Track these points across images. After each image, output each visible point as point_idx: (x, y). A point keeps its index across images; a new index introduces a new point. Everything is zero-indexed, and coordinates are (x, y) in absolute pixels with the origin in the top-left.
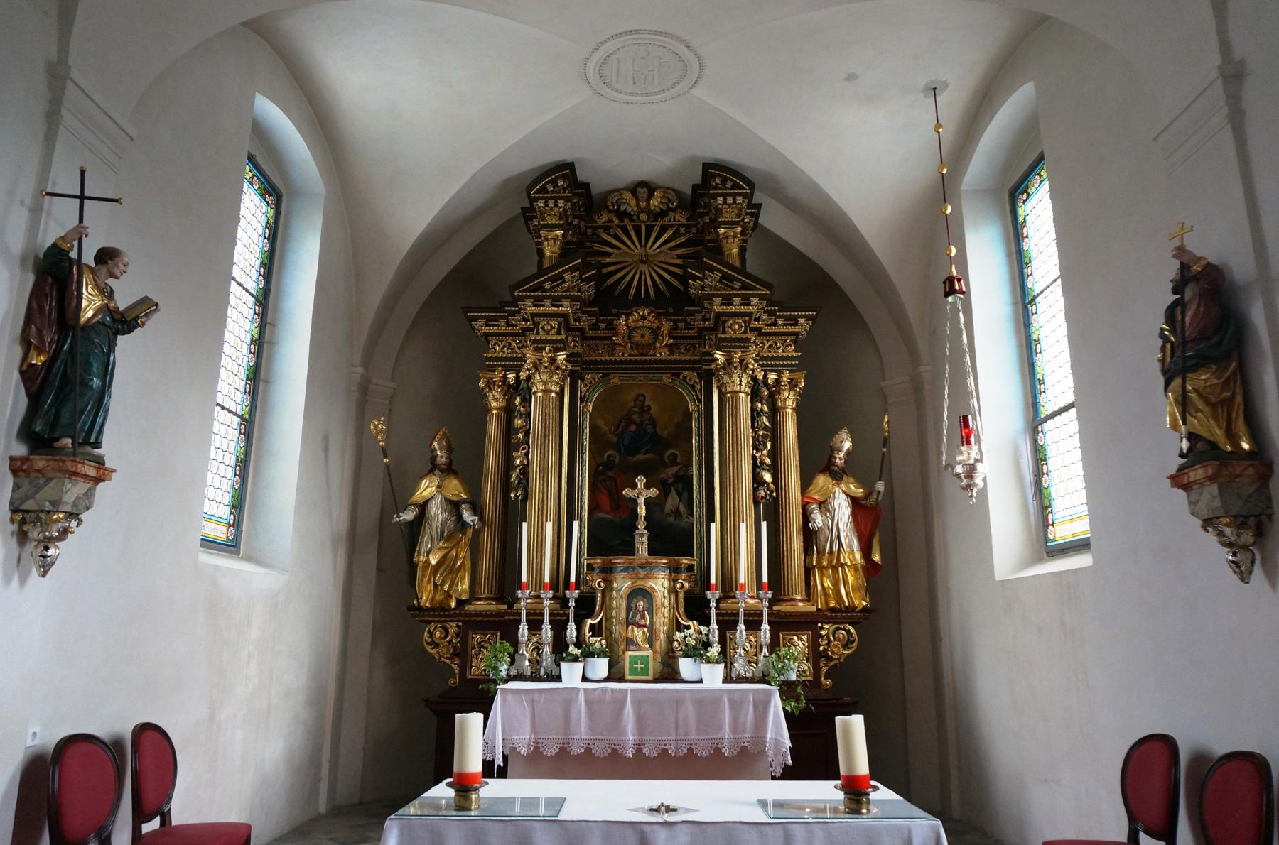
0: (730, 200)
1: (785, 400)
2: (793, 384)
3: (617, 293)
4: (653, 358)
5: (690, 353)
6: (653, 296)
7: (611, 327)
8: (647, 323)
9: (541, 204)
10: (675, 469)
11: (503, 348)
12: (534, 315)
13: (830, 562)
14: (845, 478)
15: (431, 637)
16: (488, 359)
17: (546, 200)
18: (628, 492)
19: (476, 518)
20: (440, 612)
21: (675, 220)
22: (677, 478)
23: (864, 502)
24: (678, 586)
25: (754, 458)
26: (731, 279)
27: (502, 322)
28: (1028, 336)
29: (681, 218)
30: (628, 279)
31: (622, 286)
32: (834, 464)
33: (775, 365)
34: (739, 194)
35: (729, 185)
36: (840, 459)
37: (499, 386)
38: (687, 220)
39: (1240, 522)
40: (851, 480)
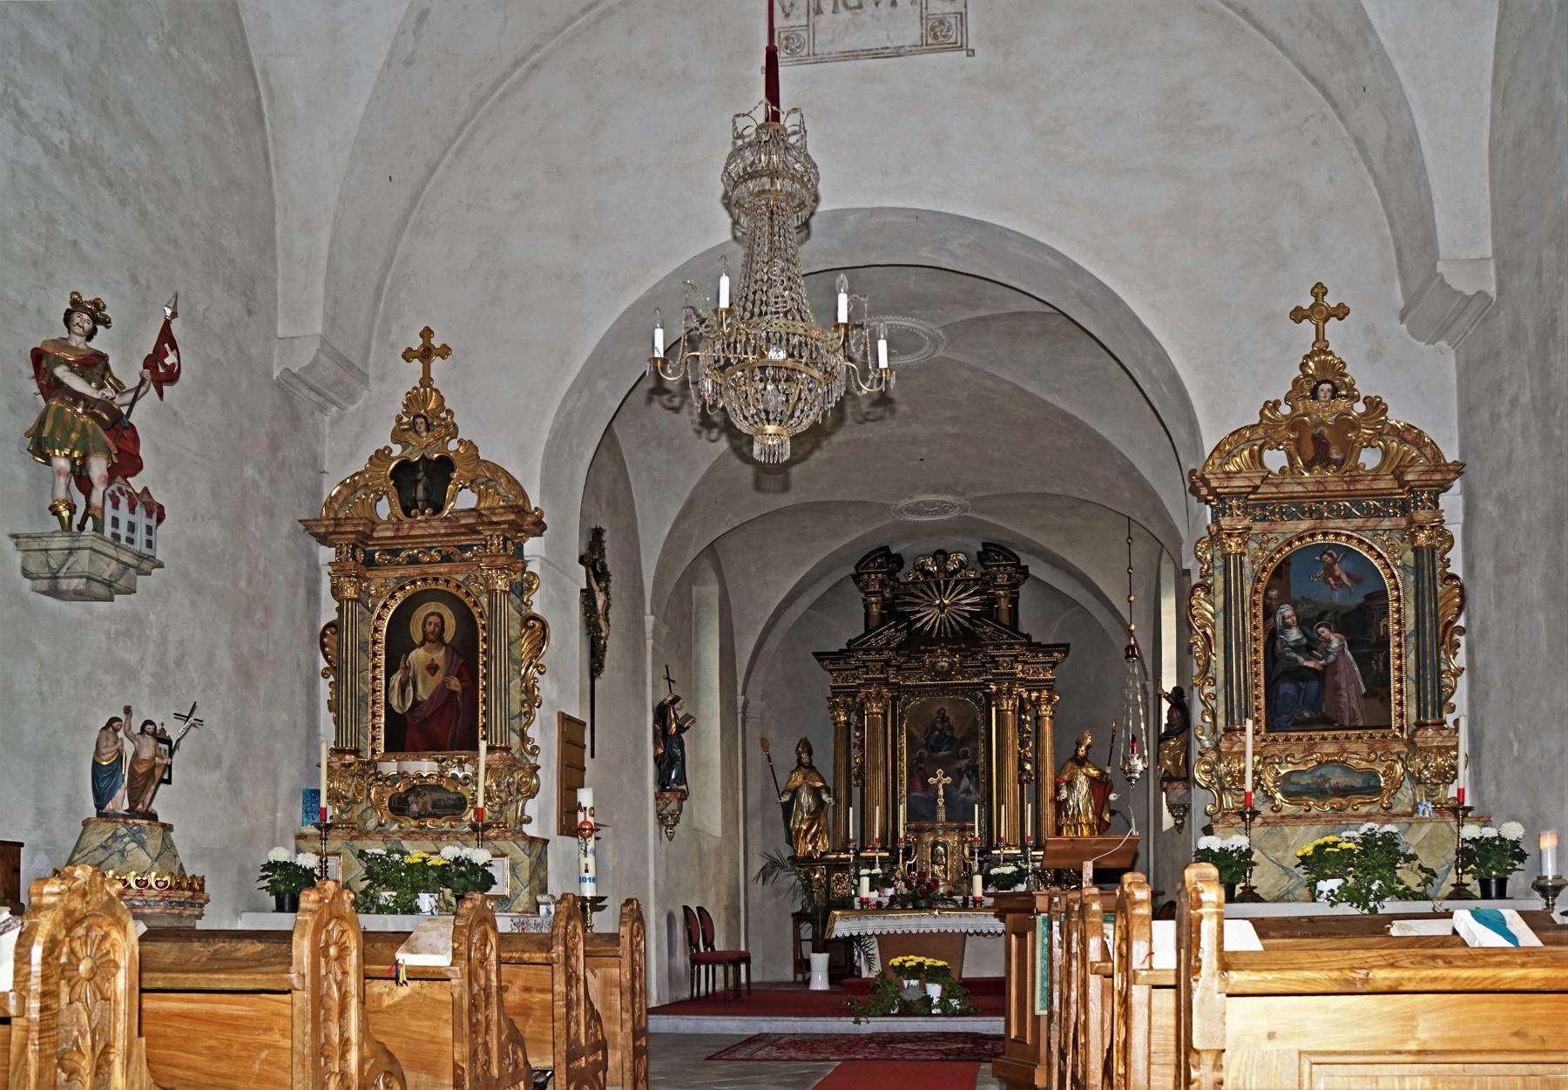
2: (1050, 700)
12: (864, 661)
17: (869, 573)
18: (932, 780)
22: (968, 767)
31: (927, 628)
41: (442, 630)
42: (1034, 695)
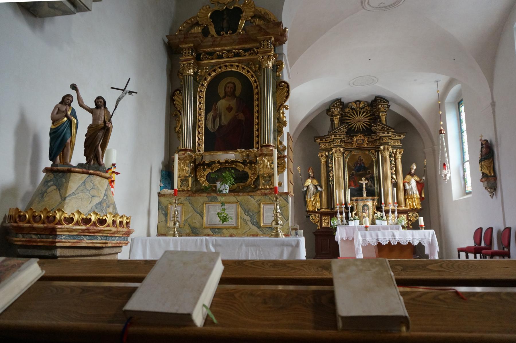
0: (383, 106)
1: (398, 156)
3: (352, 130)
4: (363, 147)
5: (373, 145)
6: (362, 130)
7: (352, 139)
8: (361, 138)
9: (333, 109)
10: (370, 175)
11: (324, 146)
13: (411, 197)
14: (414, 176)
15: (312, 218)
16: (320, 149)
17: (335, 108)
18: (360, 182)
19: (322, 189)
20: (314, 212)
21: (367, 109)
22: (370, 177)
23: (420, 182)
24: (374, 204)
25: (391, 172)
26: (384, 128)
27: (324, 140)
28: (462, 141)
29: (368, 108)
30: (355, 126)
31: (353, 128)
32: (411, 173)
33: (395, 148)
34: (385, 104)
35: (382, 102)
36: (413, 171)
37: (324, 156)
38: (370, 109)
39: (491, 188)
40: (416, 176)
41: (235, 90)
42: (395, 151)
